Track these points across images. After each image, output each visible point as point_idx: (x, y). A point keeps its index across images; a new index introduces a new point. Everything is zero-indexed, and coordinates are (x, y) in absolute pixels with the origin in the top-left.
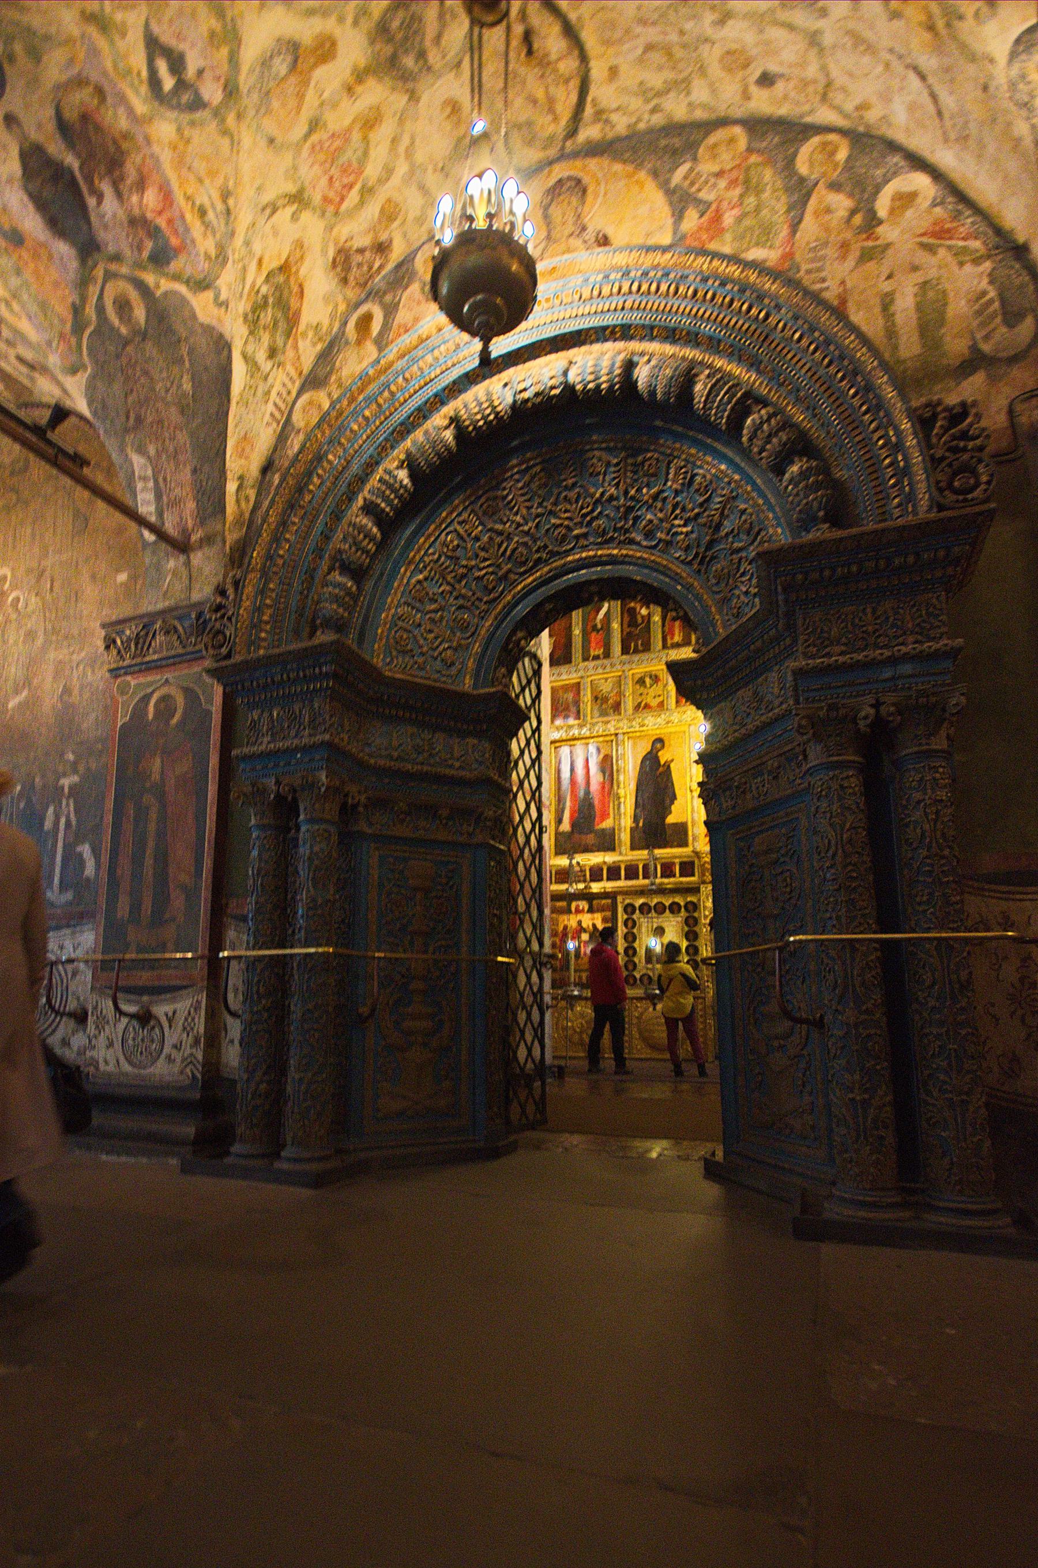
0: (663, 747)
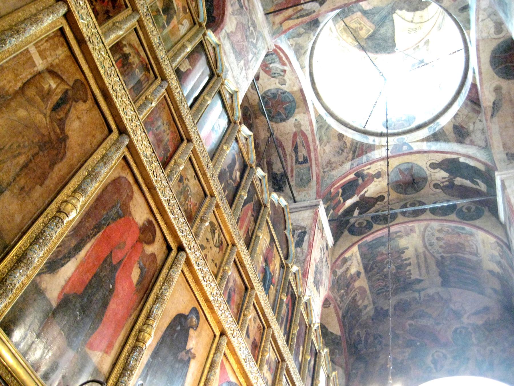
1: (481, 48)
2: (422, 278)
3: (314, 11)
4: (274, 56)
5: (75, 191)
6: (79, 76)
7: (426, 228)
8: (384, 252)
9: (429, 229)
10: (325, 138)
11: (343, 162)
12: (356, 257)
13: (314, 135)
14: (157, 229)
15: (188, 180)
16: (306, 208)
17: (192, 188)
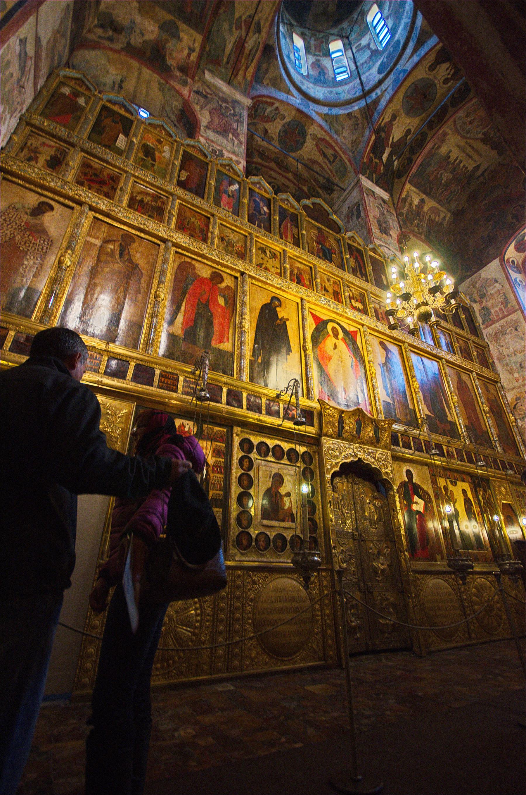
0: (280, 305)
2: (478, 164)
4: (261, 105)
5: (158, 285)
6: (121, 233)
7: (455, 123)
8: (433, 169)
9: (457, 122)
10: (339, 128)
11: (363, 133)
12: (412, 191)
13: (329, 134)
14: (221, 272)
15: (228, 236)
16: (353, 188)
17: (234, 239)
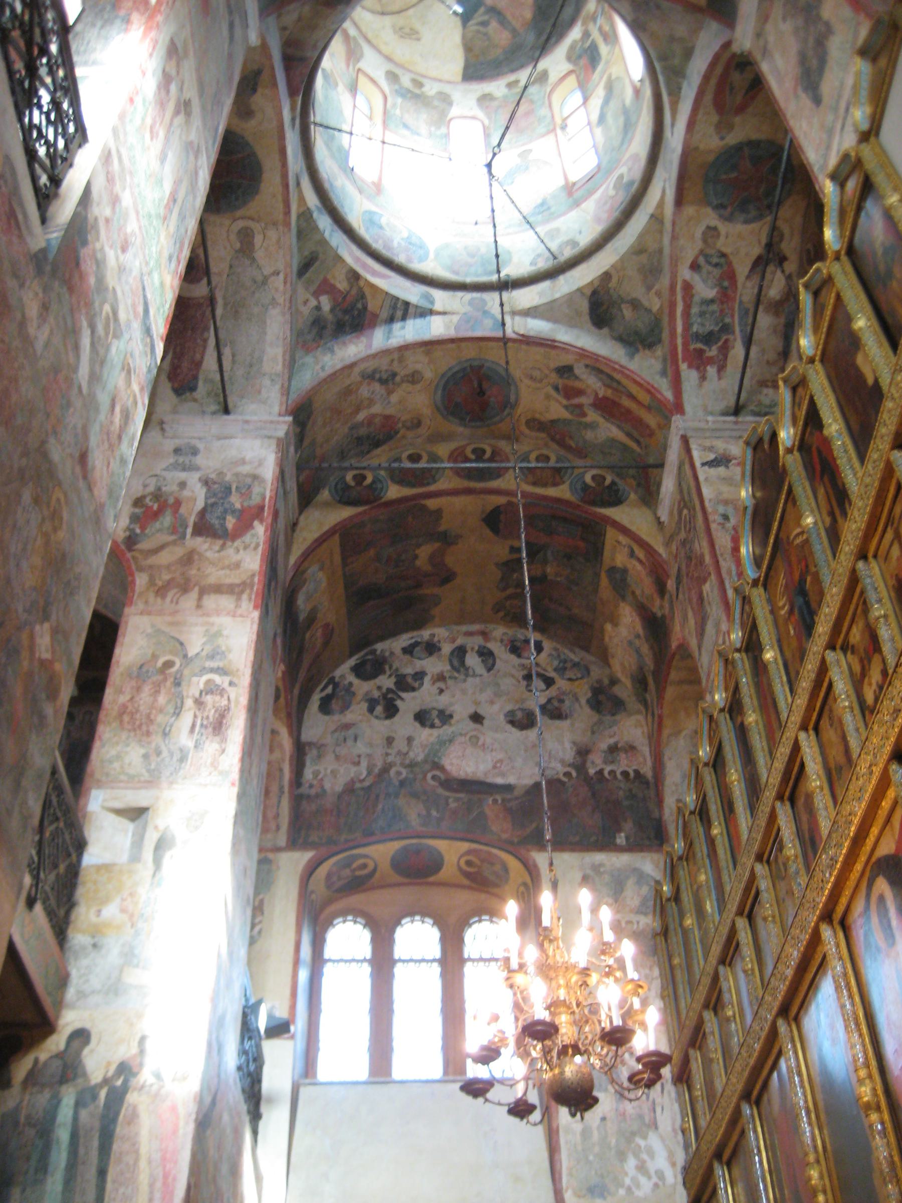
1: (281, 206)
3: (587, 366)
